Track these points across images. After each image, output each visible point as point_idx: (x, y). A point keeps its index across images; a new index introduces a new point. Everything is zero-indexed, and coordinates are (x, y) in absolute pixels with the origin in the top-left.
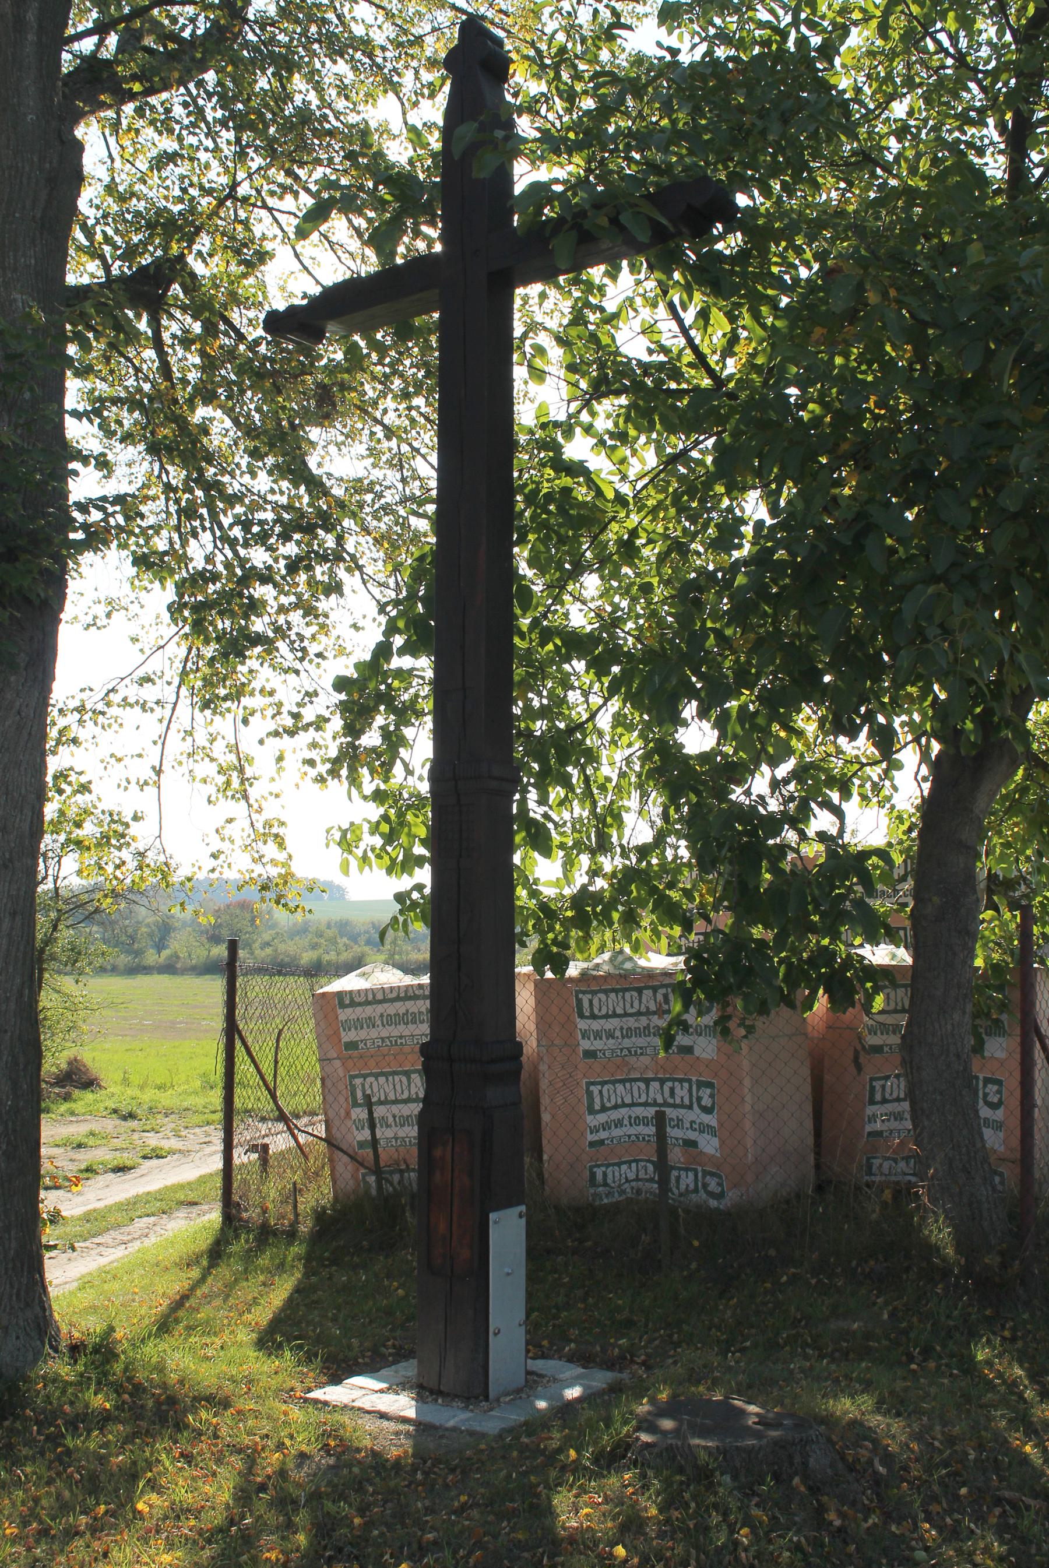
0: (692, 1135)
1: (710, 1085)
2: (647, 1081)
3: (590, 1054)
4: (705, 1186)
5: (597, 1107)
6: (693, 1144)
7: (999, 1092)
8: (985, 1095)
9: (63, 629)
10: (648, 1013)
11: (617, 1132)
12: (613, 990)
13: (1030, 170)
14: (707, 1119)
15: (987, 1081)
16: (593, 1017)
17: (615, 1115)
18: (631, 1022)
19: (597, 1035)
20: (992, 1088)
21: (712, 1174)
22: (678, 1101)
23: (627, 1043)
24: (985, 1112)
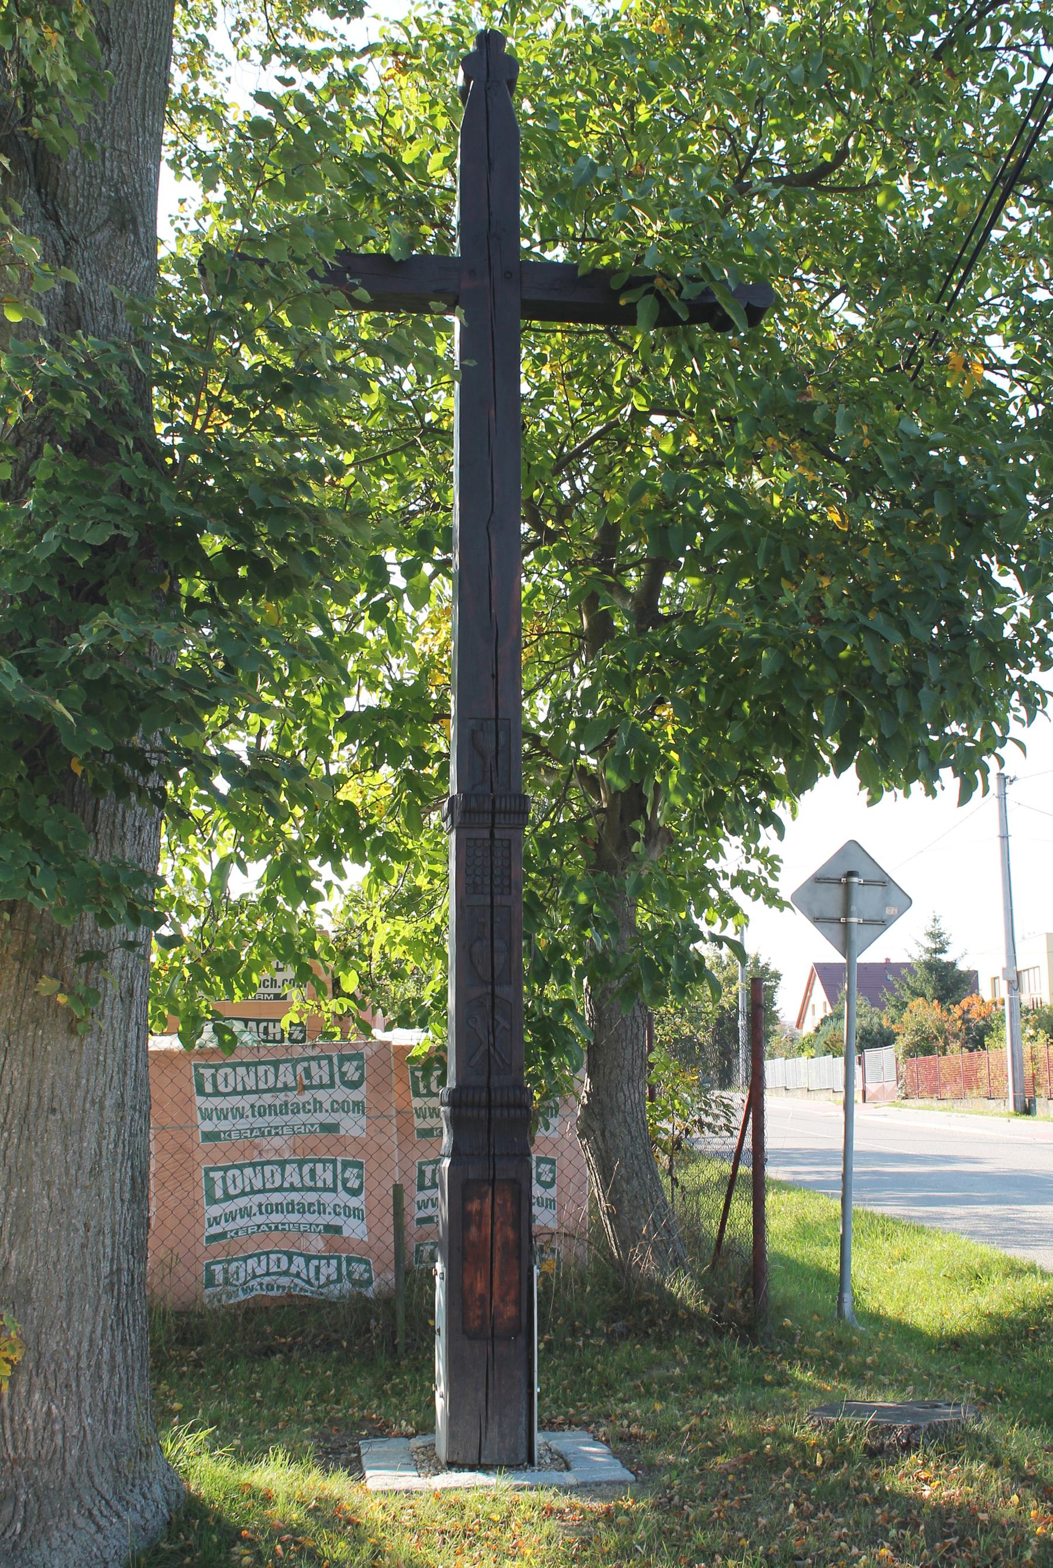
0: (337, 1221)
1: (359, 1165)
2: (282, 1164)
3: (211, 1136)
4: (350, 1274)
5: (219, 1193)
6: (338, 1230)
7: (552, 1171)
8: (539, 1175)
9: (767, 1093)
10: (286, 1088)
11: (240, 1222)
12: (241, 1064)
13: (676, 714)
14: (354, 1202)
15: (540, 1161)
16: (217, 1093)
17: (242, 1202)
18: (268, 1099)
19: (223, 1115)
20: (545, 1167)
21: (360, 1261)
22: (320, 1184)
23: (260, 1122)
24: (537, 1191)
